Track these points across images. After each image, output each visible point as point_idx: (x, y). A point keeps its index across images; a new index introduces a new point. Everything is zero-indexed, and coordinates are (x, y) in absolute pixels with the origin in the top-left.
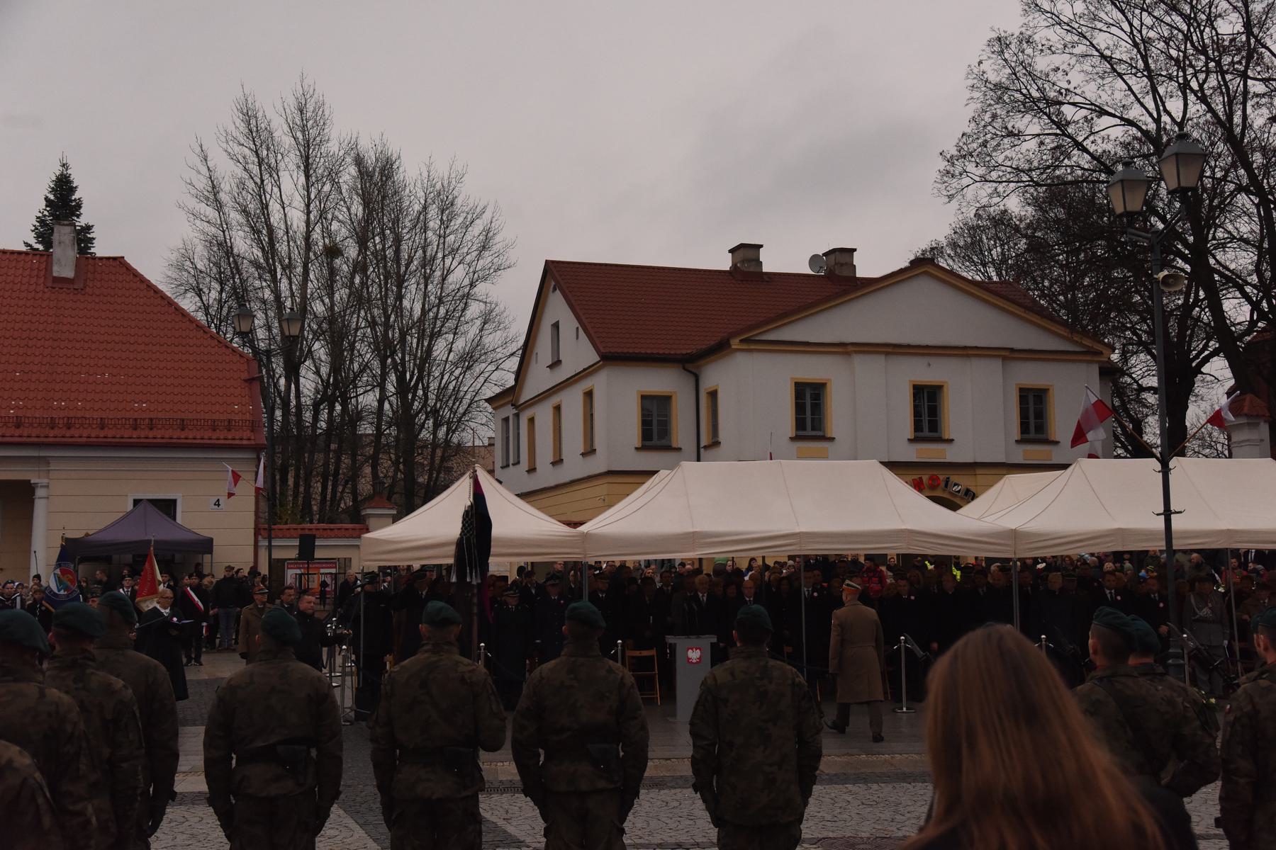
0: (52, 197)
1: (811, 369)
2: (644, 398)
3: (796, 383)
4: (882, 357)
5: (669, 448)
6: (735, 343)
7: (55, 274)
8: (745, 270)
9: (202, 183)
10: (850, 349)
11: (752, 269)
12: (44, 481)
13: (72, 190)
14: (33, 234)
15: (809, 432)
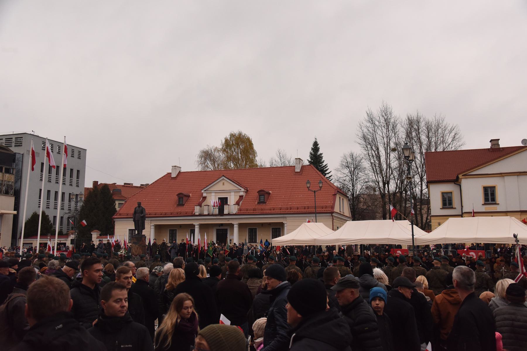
0: (313, 147)
1: (489, 182)
2: (442, 193)
3: (484, 187)
4: (516, 177)
5: (452, 208)
6: (460, 176)
7: (296, 171)
8: (493, 148)
9: (360, 135)
10: (503, 175)
11: (496, 147)
12: (286, 222)
13: (318, 145)
14: (309, 157)
15: (490, 202)
